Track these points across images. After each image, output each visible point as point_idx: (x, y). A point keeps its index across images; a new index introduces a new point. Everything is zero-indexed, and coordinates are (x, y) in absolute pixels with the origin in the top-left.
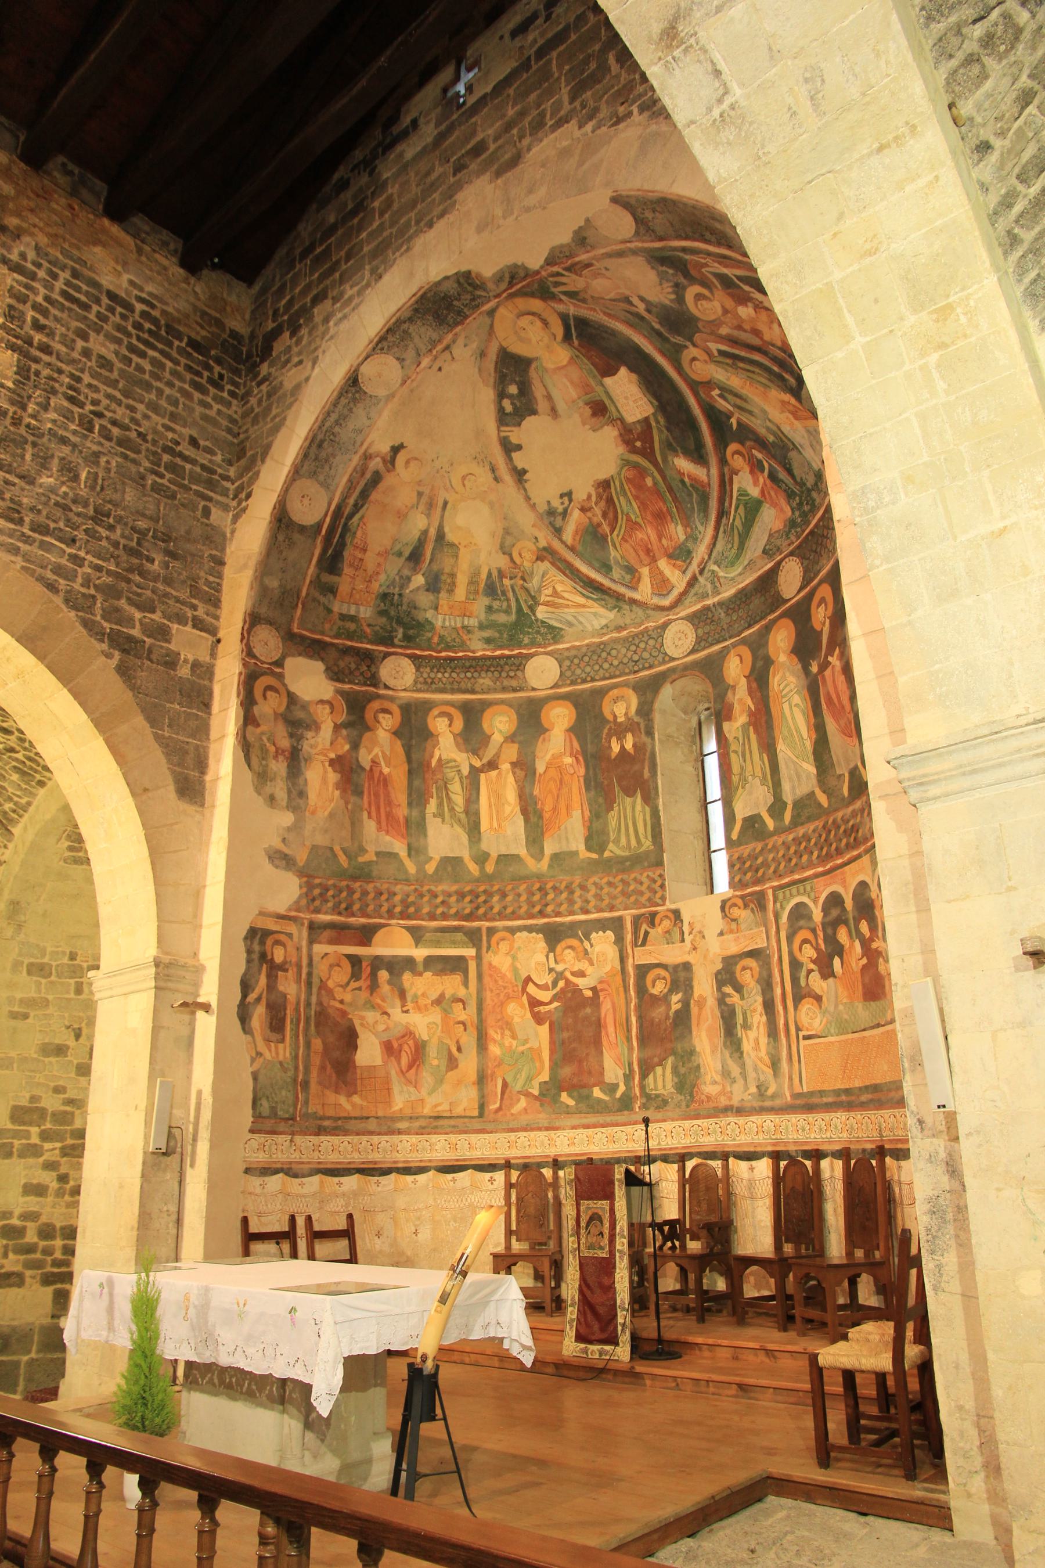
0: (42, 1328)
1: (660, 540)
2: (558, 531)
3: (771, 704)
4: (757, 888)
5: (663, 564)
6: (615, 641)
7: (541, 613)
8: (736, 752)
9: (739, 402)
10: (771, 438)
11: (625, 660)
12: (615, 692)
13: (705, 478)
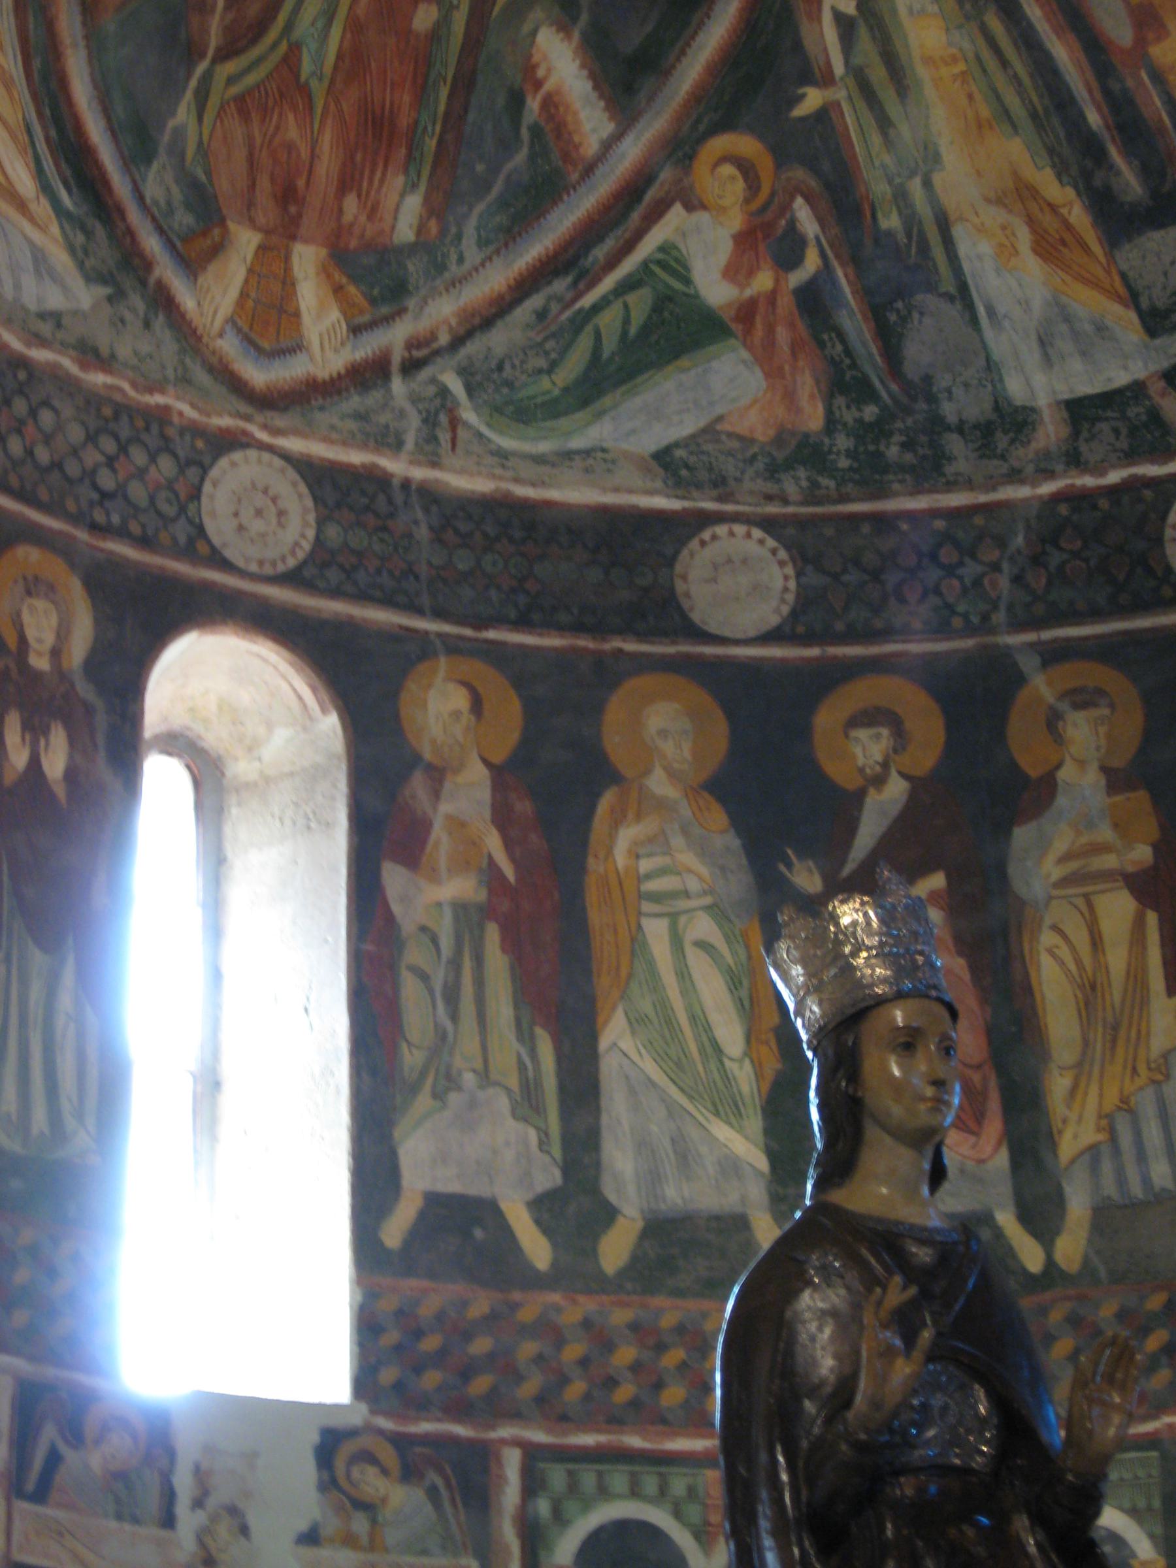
1: (343, 187)
3: (592, 896)
4: (460, 1430)
5: (306, 259)
8: (424, 977)
9: (878, 74)
10: (891, 221)
11: (72, 469)
12: (29, 555)
13: (591, 147)
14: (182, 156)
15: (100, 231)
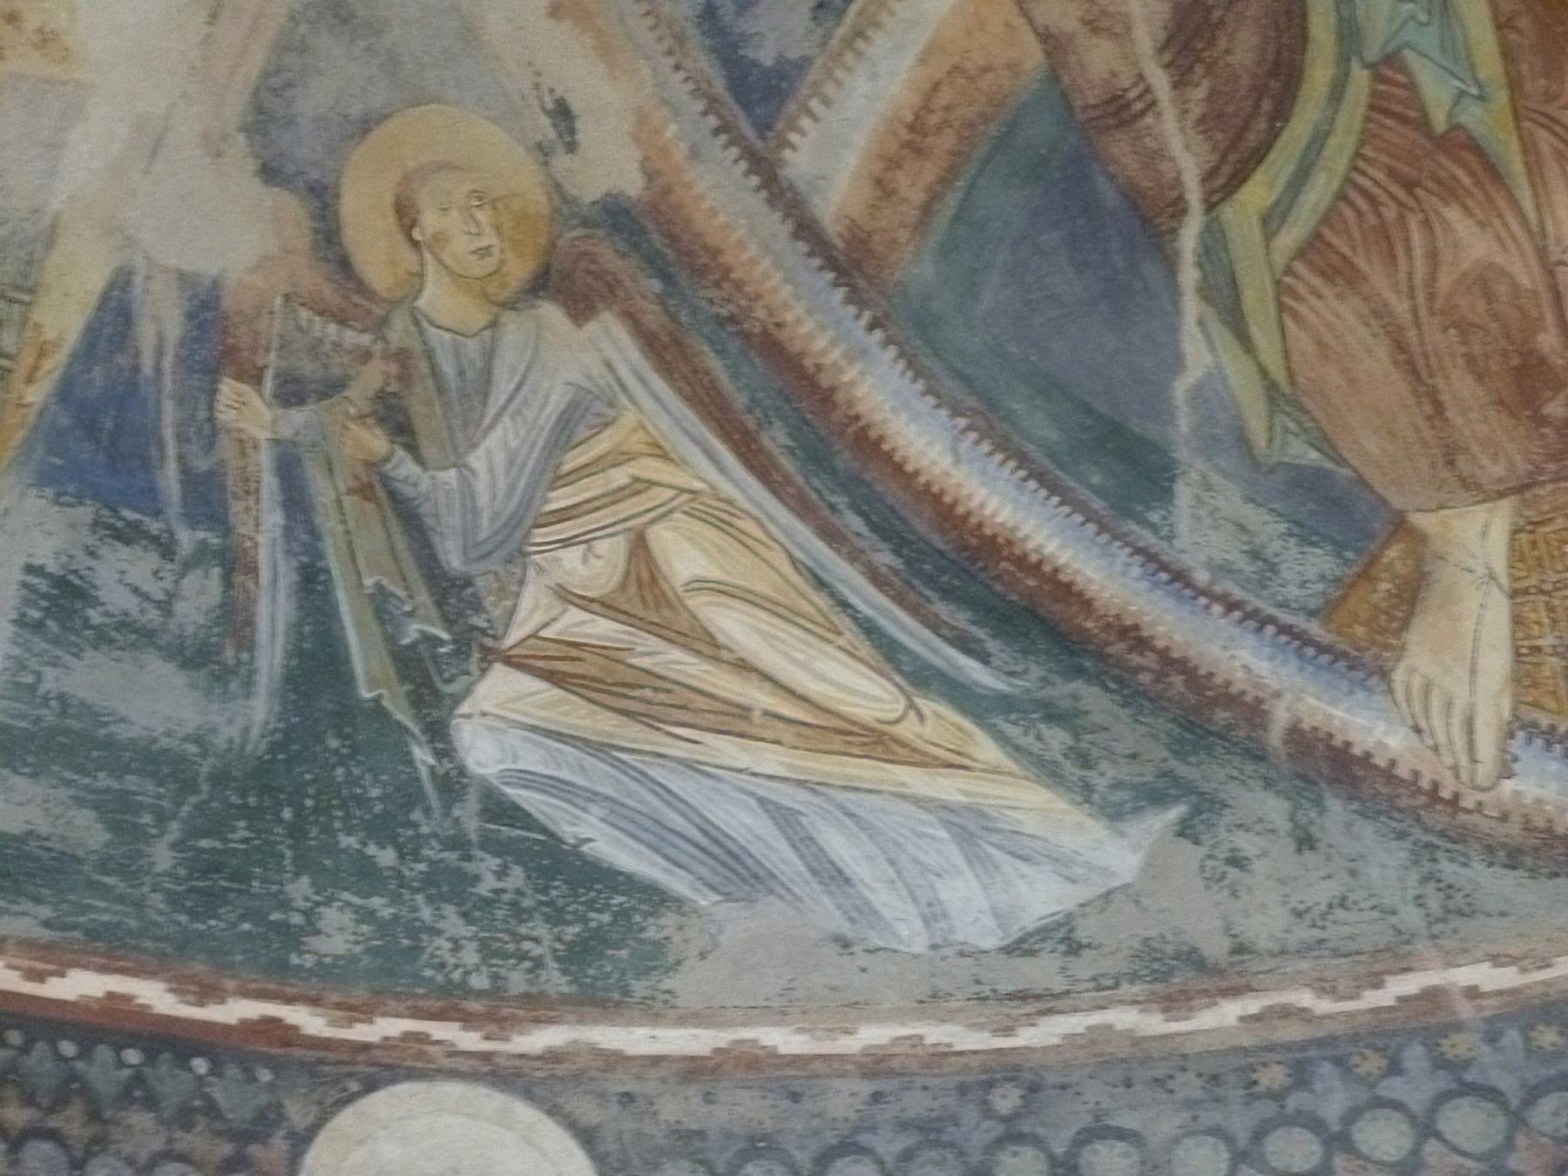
2: (757, 99)
6: (1132, 1066)
7: (500, 728)
14: (1242, 439)
15: (1094, 699)
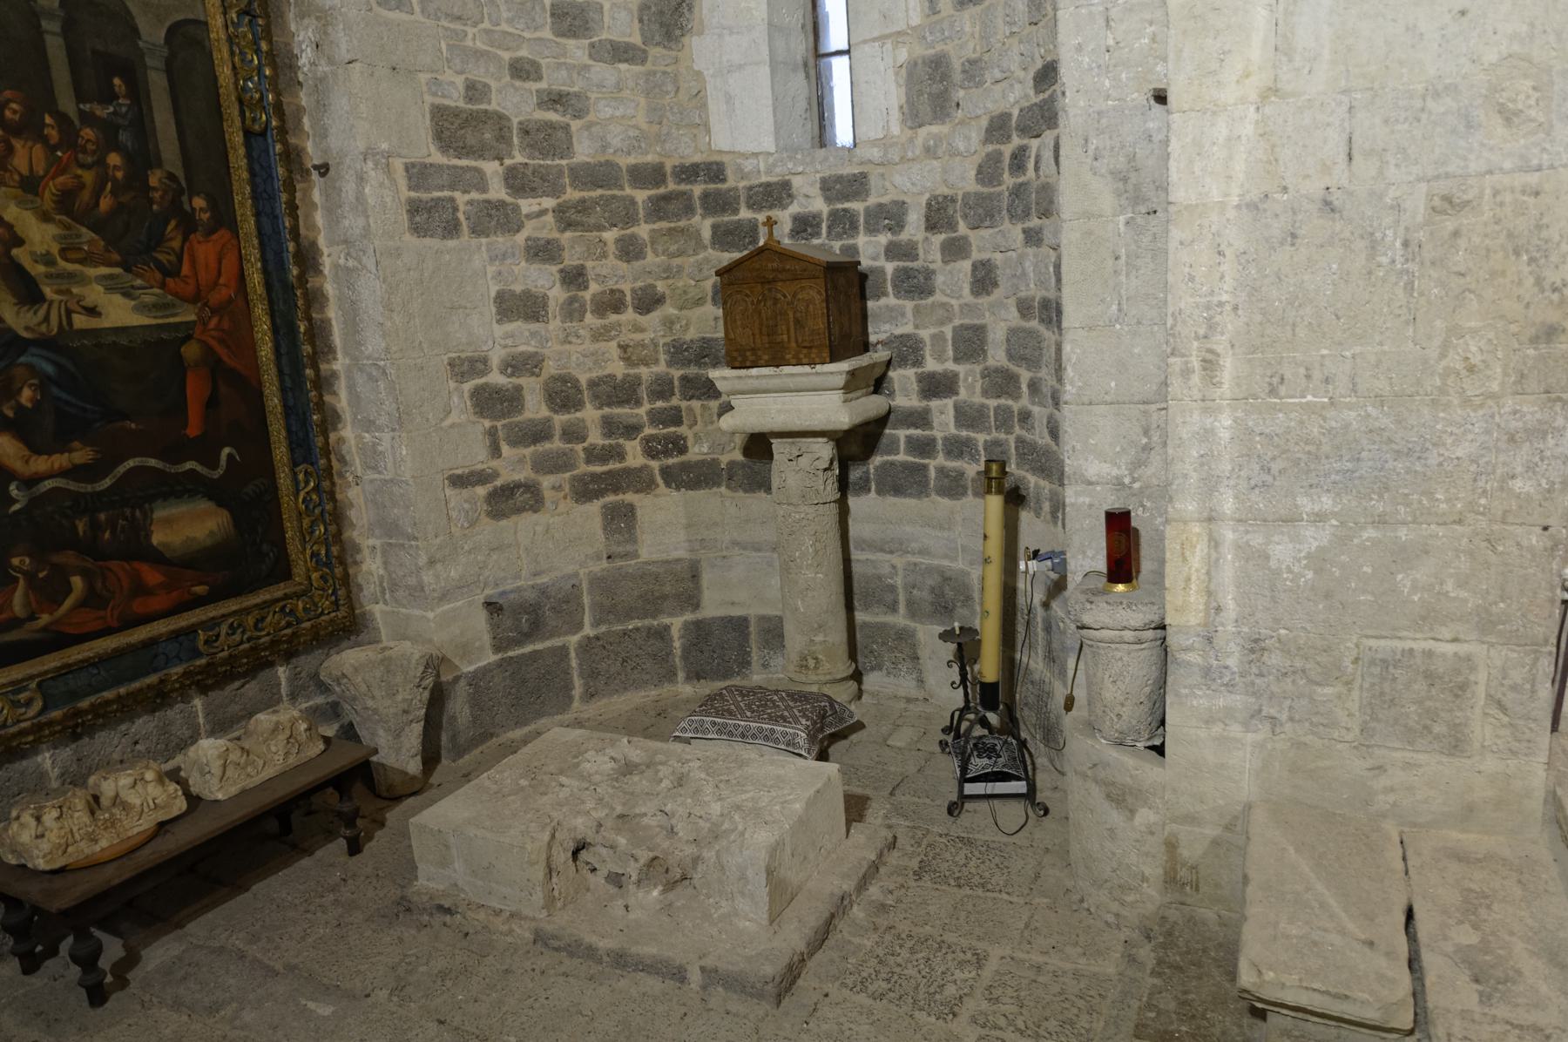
0: (597, 582)
